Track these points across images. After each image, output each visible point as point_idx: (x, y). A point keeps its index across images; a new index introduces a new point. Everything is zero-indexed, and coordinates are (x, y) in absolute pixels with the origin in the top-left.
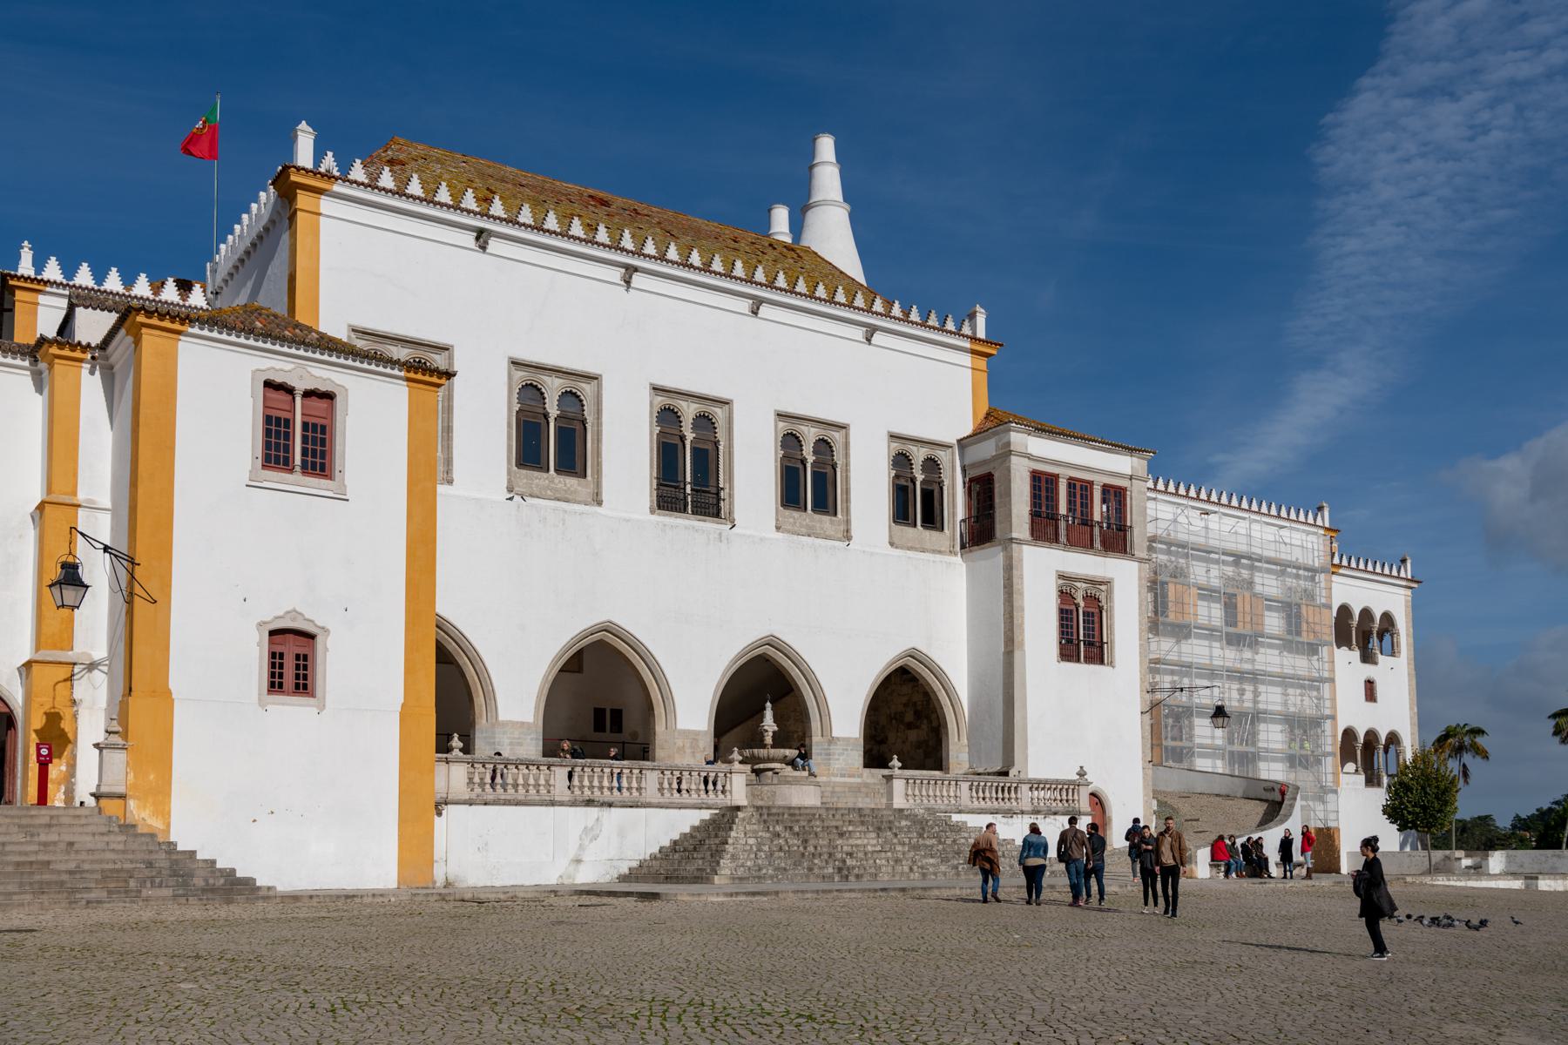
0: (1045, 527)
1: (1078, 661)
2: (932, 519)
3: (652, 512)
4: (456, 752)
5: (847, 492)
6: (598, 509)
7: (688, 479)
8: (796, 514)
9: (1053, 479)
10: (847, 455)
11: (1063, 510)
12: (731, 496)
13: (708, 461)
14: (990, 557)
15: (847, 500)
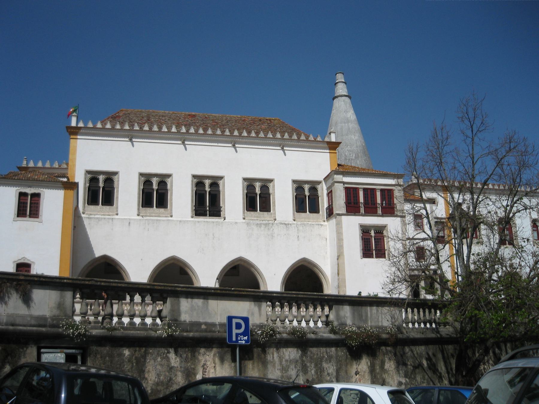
0: (352, 208)
1: (373, 257)
2: (315, 209)
3: (192, 217)
4: (78, 300)
5: (274, 203)
6: (170, 218)
7: (208, 204)
8: (252, 213)
9: (356, 190)
10: (274, 190)
11: (362, 200)
12: (224, 209)
13: (215, 198)
14: (333, 221)
15: (274, 206)
